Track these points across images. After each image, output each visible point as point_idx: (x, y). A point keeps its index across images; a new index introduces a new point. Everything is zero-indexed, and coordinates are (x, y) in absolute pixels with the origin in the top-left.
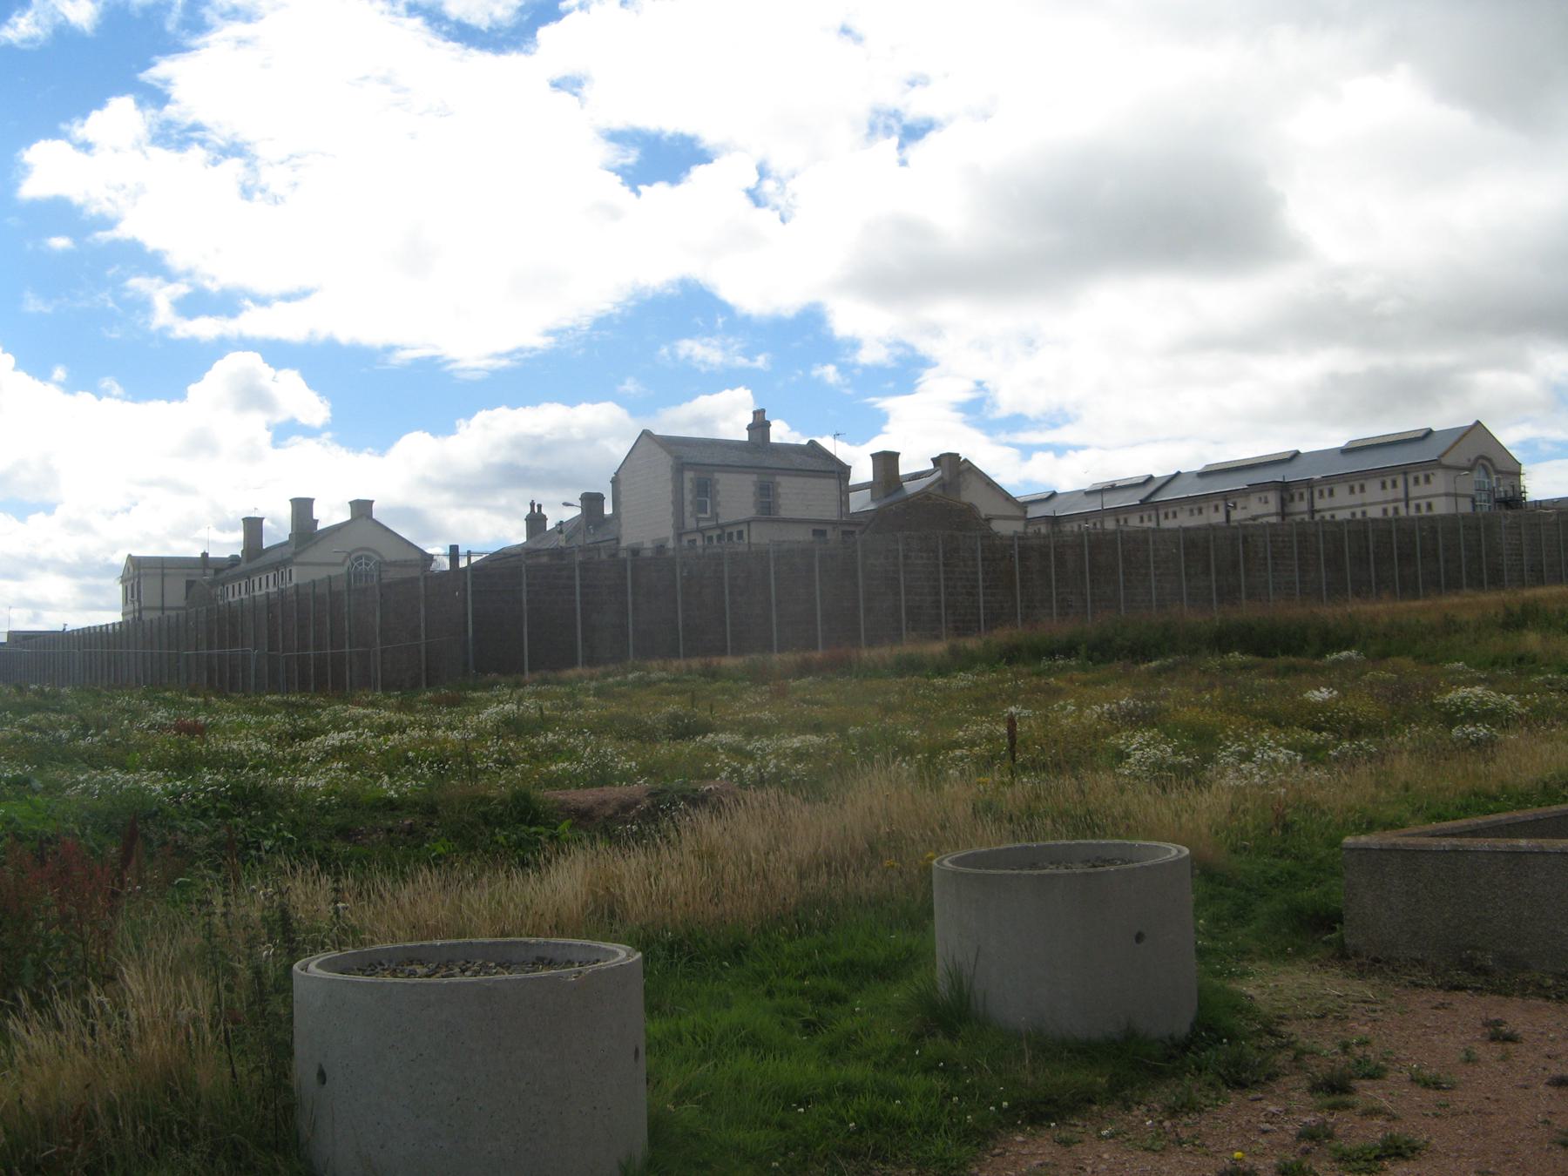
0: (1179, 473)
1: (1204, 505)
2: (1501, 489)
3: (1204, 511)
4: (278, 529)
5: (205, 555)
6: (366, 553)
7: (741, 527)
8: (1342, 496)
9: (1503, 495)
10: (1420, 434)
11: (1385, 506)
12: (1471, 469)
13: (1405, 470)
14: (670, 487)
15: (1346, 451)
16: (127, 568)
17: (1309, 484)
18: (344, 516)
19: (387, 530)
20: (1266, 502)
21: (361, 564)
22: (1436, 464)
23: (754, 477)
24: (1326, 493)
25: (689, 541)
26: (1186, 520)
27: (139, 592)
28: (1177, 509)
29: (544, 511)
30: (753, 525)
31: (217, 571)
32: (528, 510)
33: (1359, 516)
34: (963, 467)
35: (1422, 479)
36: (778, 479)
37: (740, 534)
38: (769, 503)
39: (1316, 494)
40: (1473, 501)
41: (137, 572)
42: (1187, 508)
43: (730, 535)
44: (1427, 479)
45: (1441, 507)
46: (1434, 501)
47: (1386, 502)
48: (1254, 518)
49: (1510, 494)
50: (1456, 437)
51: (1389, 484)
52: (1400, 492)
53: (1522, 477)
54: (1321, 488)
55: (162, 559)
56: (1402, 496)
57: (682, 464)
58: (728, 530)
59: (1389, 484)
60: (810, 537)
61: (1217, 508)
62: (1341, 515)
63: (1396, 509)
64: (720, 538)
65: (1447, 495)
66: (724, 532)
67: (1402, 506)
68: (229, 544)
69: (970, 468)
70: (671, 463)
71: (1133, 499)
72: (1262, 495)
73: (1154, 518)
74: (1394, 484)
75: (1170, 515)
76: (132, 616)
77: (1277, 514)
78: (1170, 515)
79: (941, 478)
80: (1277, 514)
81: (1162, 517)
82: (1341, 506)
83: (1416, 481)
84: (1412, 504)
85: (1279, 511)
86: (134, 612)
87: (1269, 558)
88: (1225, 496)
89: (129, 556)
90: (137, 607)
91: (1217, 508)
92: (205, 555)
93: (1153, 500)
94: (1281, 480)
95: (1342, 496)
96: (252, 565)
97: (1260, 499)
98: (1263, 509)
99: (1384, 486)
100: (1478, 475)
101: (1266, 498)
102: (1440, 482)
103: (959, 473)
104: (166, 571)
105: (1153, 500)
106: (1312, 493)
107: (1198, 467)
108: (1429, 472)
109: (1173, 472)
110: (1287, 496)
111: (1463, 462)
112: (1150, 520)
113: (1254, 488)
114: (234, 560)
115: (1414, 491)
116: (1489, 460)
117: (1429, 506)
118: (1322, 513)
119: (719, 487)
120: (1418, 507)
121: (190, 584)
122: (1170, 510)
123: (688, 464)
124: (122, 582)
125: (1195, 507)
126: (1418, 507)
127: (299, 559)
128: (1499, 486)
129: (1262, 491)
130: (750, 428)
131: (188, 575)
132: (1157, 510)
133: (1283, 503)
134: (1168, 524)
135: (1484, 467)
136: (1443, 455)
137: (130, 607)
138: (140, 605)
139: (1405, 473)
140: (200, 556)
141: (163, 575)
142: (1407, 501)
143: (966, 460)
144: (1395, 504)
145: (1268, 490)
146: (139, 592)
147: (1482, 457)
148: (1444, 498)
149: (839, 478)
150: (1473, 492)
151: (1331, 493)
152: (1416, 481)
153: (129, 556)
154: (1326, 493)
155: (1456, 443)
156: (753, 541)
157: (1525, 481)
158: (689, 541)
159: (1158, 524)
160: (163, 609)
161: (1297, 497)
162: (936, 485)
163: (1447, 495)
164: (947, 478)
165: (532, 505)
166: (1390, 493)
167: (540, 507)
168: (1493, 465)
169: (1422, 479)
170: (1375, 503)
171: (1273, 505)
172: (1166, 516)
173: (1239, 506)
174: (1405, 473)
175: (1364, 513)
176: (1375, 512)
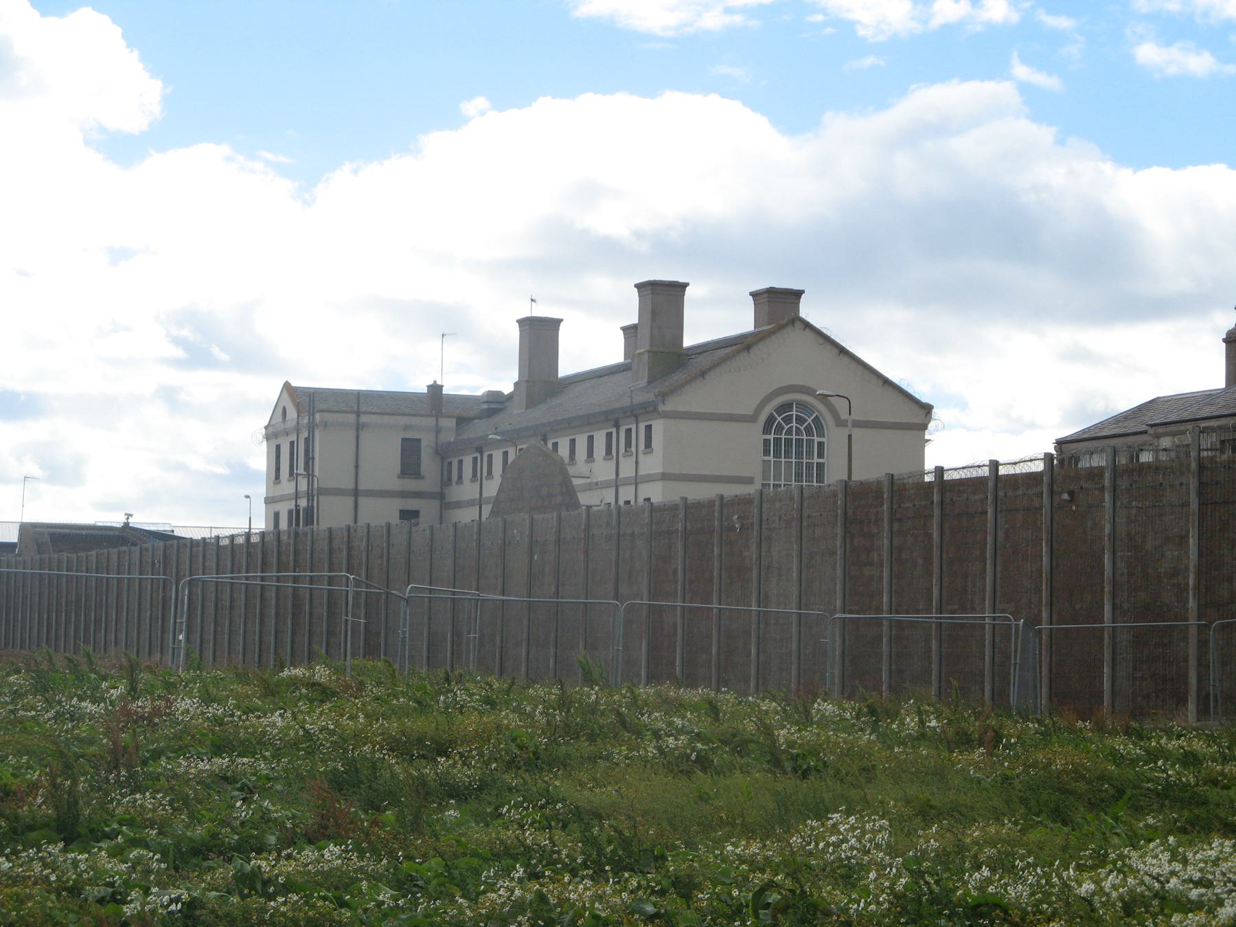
5: (435, 389)
16: (280, 411)
18: (742, 320)
19: (843, 351)
21: (788, 420)
27: (309, 459)
31: (462, 421)
41: (305, 421)
55: (359, 396)
76: (292, 505)
86: (297, 496)
89: (287, 386)
90: (303, 485)
92: (435, 389)
96: (538, 415)
104: (364, 419)
114: (494, 404)
121: (410, 451)
124: (268, 437)
127: (670, 406)
131: (407, 428)
137: (287, 487)
140: (425, 391)
141: (359, 428)
153: (287, 386)
160: (356, 493)
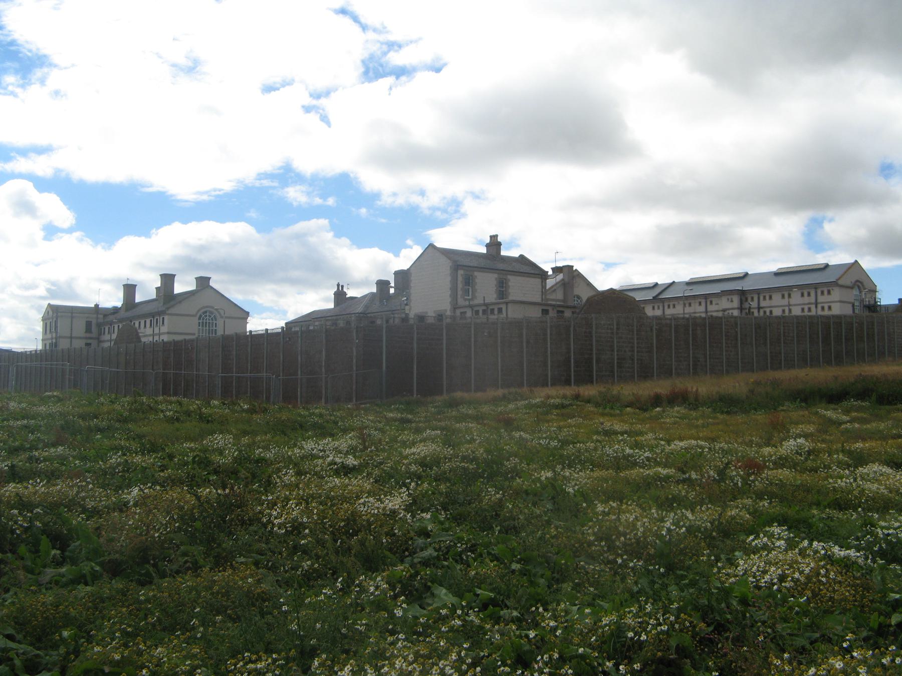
0: (674, 282)
1: (692, 301)
2: (867, 300)
3: (692, 305)
4: (147, 291)
6: (211, 310)
7: (500, 306)
8: (777, 299)
9: (867, 303)
10: (822, 267)
11: (783, 308)
12: (852, 288)
13: (815, 286)
14: (449, 279)
15: (777, 274)
16: (47, 312)
17: (758, 292)
18: (192, 287)
19: (223, 296)
20: (732, 301)
21: (206, 316)
22: (835, 284)
23: (496, 276)
24: (767, 298)
25: (461, 313)
26: (678, 310)
27: (56, 327)
28: (676, 303)
29: (345, 290)
30: (510, 305)
31: (105, 316)
32: (336, 290)
33: (768, 314)
34: (575, 274)
35: (826, 292)
36: (509, 277)
37: (500, 310)
38: (503, 291)
39: (761, 298)
40: (853, 306)
41: (55, 315)
42: (682, 302)
43: (492, 311)
44: (829, 292)
45: (837, 310)
46: (833, 305)
47: (804, 304)
48: (724, 310)
49: (872, 302)
50: (844, 270)
51: (806, 294)
52: (812, 299)
53: (877, 293)
54: (764, 294)
56: (813, 300)
57: (458, 266)
58: (491, 307)
59: (806, 294)
60: (539, 314)
61: (700, 304)
62: (777, 312)
63: (810, 310)
64: (484, 312)
65: (841, 302)
66: (488, 308)
67: (813, 307)
68: (113, 299)
69: (578, 275)
70: (451, 264)
71: (649, 296)
72: (730, 297)
73: (661, 308)
74: (809, 294)
75: (671, 306)
76: (50, 341)
77: (738, 308)
78: (671, 306)
79: (563, 280)
80: (738, 308)
81: (666, 307)
82: (776, 306)
83: (822, 293)
84: (819, 306)
85: (739, 306)
86: (52, 339)
87: (795, 337)
88: (706, 297)
89: (49, 304)
90: (54, 335)
91: (700, 304)
92: (97, 306)
93: (661, 297)
94: (741, 289)
95: (777, 299)
96: (129, 314)
97: (728, 299)
98: (731, 306)
99: (802, 295)
100: (856, 292)
101: (732, 299)
102: (836, 294)
103: (573, 277)
105: (661, 297)
106: (759, 298)
107: (687, 279)
108: (830, 289)
109: (671, 281)
110: (744, 299)
111: (849, 283)
112: (659, 308)
113: (724, 293)
114: (115, 310)
115: (821, 299)
116: (861, 283)
117: (830, 308)
118: (765, 309)
119: (477, 281)
120: (823, 308)
121: (89, 325)
122: (671, 304)
123: (460, 265)
124: (43, 320)
125: (687, 302)
126: (823, 308)
127: (169, 312)
128: (866, 298)
129: (730, 295)
130: (488, 246)
131: (87, 318)
132: (663, 303)
133: (741, 303)
134: (669, 312)
135: (859, 287)
136: (837, 280)
137: (49, 336)
138: (56, 335)
139: (816, 288)
141: (72, 317)
142: (816, 304)
143: (576, 270)
144: (809, 306)
145: (733, 295)
146: (56, 327)
147: (857, 281)
148: (838, 304)
149: (542, 278)
150: (853, 301)
151: (771, 298)
152: (822, 293)
153: (49, 304)
154: (767, 298)
155: (845, 272)
156: (510, 316)
157: (878, 295)
158: (461, 313)
159: (664, 313)
160: (71, 338)
161: (749, 299)
162: (561, 283)
163: (841, 302)
164: (566, 280)
165: (338, 285)
166: (806, 299)
167: (342, 287)
168: (863, 286)
169: (826, 292)
170: (798, 305)
171: (736, 303)
172: (669, 306)
173: (714, 303)
174: (816, 288)
175: (771, 312)
176: (797, 311)
